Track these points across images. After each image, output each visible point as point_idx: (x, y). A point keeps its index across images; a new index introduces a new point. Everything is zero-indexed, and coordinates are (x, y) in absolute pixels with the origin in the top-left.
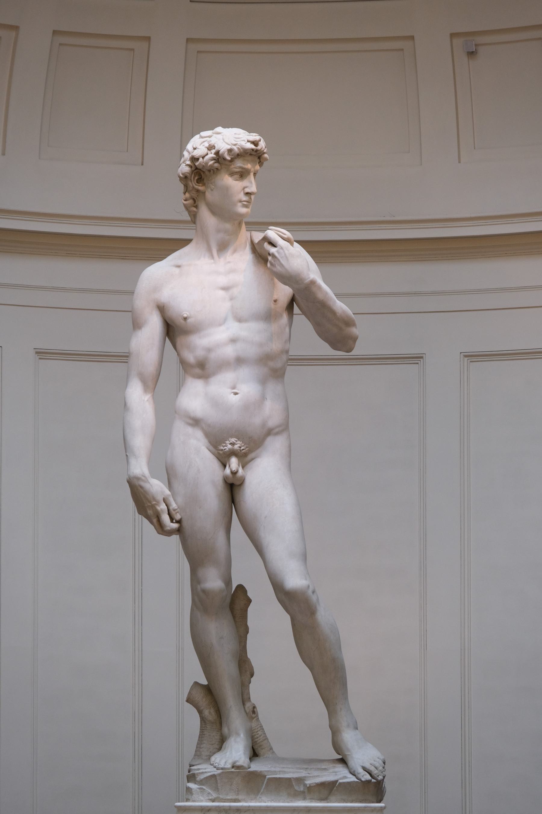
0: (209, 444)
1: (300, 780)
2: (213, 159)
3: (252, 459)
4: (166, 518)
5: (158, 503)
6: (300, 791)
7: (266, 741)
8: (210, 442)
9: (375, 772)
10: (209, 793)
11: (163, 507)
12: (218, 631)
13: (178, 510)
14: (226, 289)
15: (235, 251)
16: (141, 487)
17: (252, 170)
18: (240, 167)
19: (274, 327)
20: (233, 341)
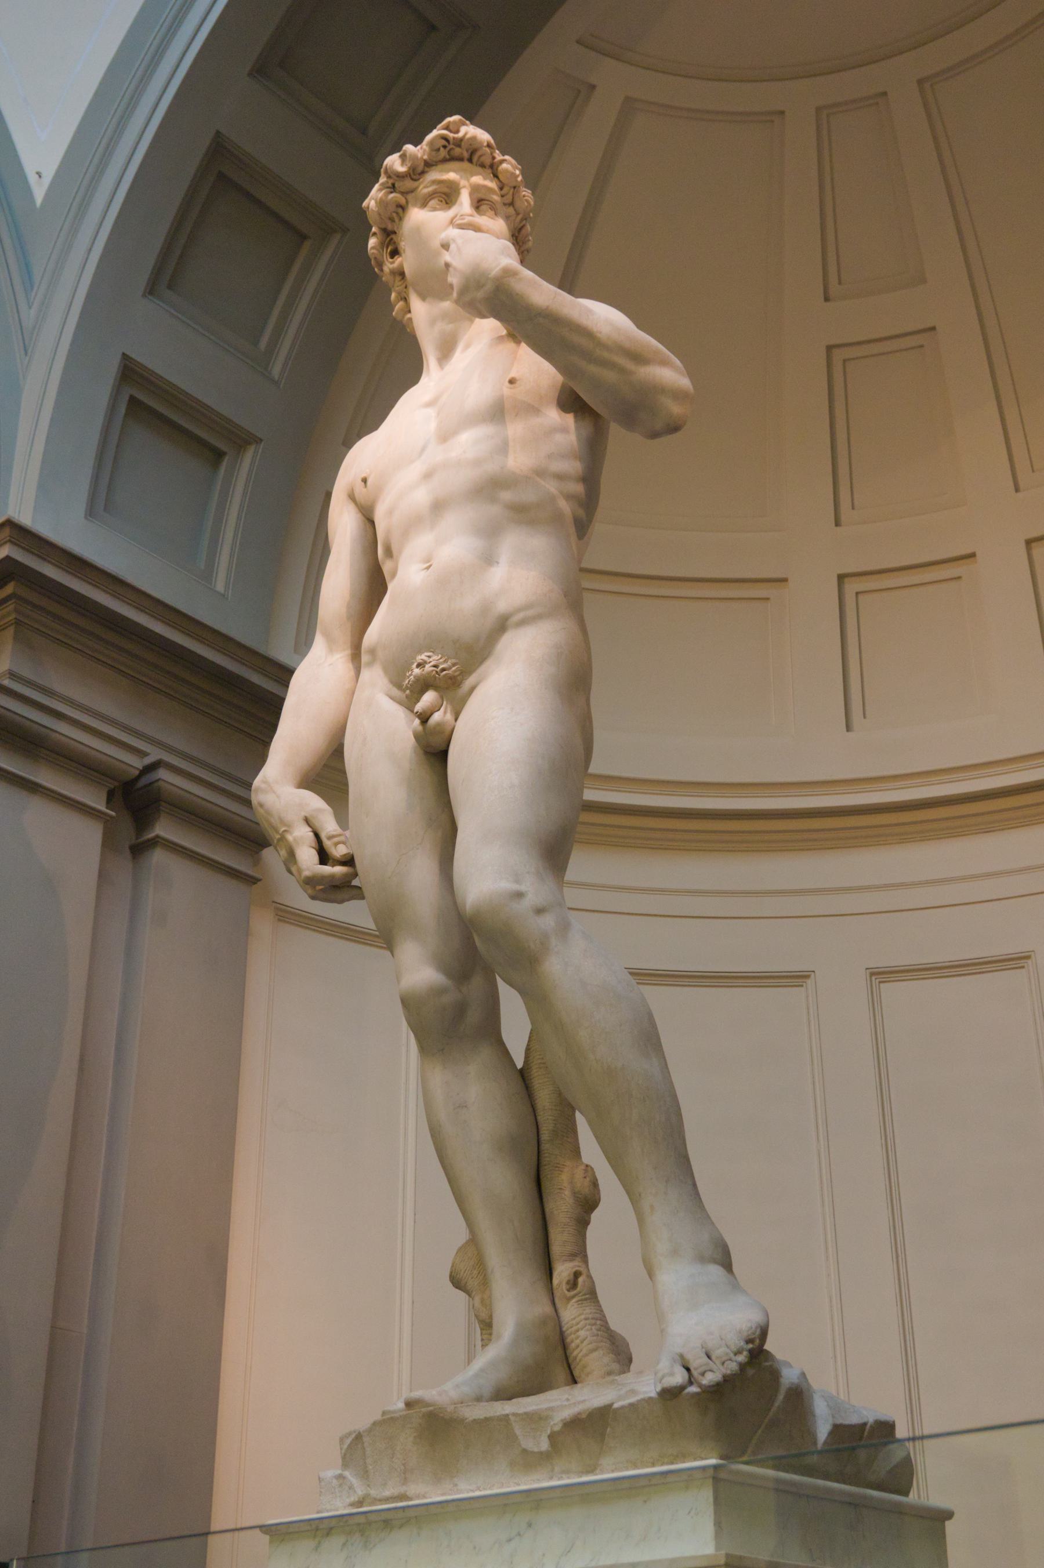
0: (391, 686)
1: (534, 1419)
2: (384, 186)
3: (472, 689)
4: (307, 857)
5: (289, 827)
6: (541, 1453)
7: (595, 1354)
8: (391, 682)
9: (697, 1362)
10: (351, 1487)
11: (301, 834)
12: (476, 1100)
13: (342, 838)
14: (430, 404)
15: (468, 346)
16: (261, 805)
17: (463, 183)
18: (434, 182)
19: (515, 429)
20: (428, 476)
